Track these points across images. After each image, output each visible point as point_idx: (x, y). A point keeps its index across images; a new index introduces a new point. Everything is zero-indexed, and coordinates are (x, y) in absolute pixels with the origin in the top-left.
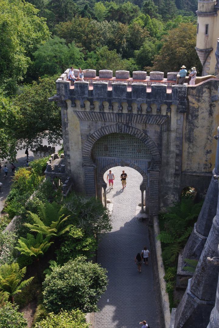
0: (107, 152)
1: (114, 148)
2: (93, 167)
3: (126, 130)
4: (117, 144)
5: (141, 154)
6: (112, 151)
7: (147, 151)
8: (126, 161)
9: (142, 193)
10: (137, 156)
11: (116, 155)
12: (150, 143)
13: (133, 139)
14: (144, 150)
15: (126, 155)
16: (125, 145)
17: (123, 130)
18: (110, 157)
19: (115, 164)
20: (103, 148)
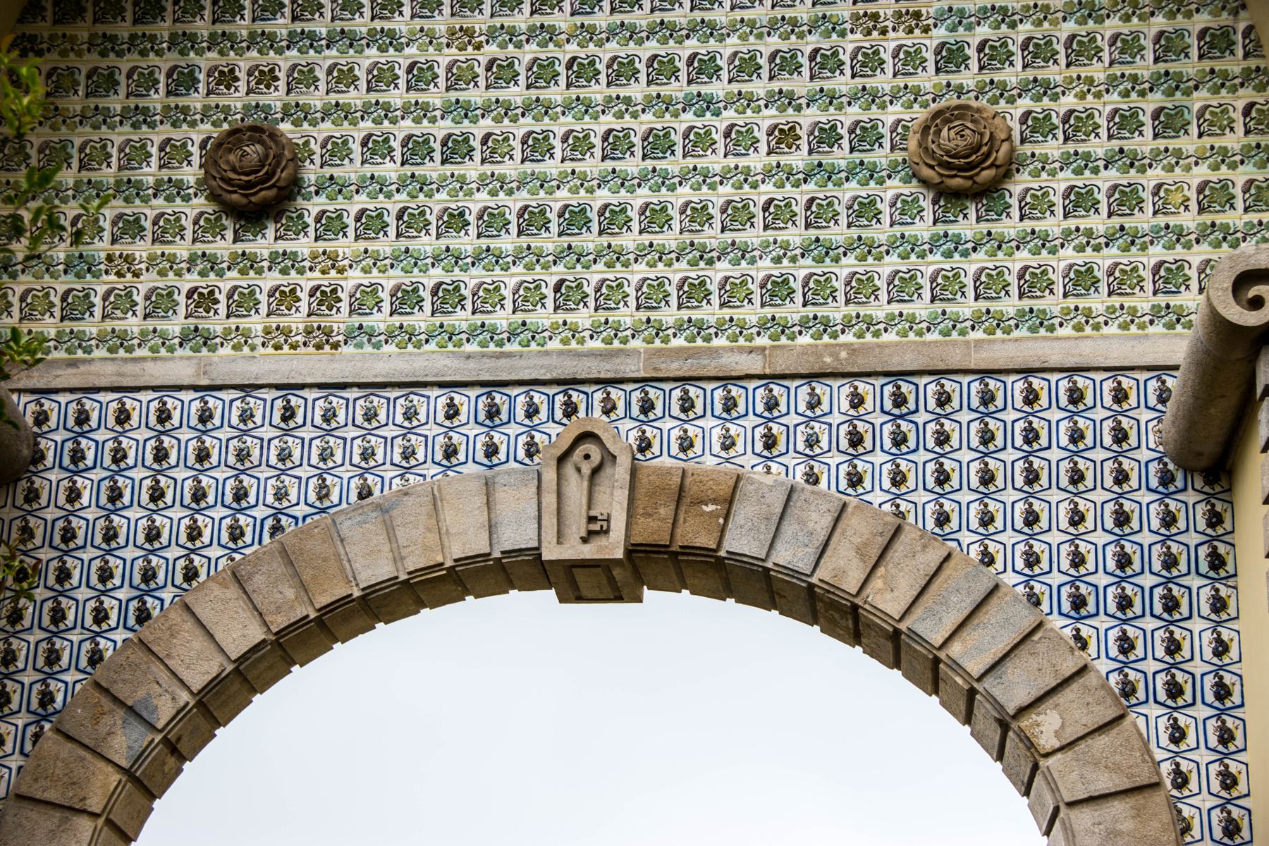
0: (264, 244)
4: (502, 72)
5: (1010, 226)
7: (1144, 143)
14: (1076, 125)
18: (324, 339)
20: (190, 174)
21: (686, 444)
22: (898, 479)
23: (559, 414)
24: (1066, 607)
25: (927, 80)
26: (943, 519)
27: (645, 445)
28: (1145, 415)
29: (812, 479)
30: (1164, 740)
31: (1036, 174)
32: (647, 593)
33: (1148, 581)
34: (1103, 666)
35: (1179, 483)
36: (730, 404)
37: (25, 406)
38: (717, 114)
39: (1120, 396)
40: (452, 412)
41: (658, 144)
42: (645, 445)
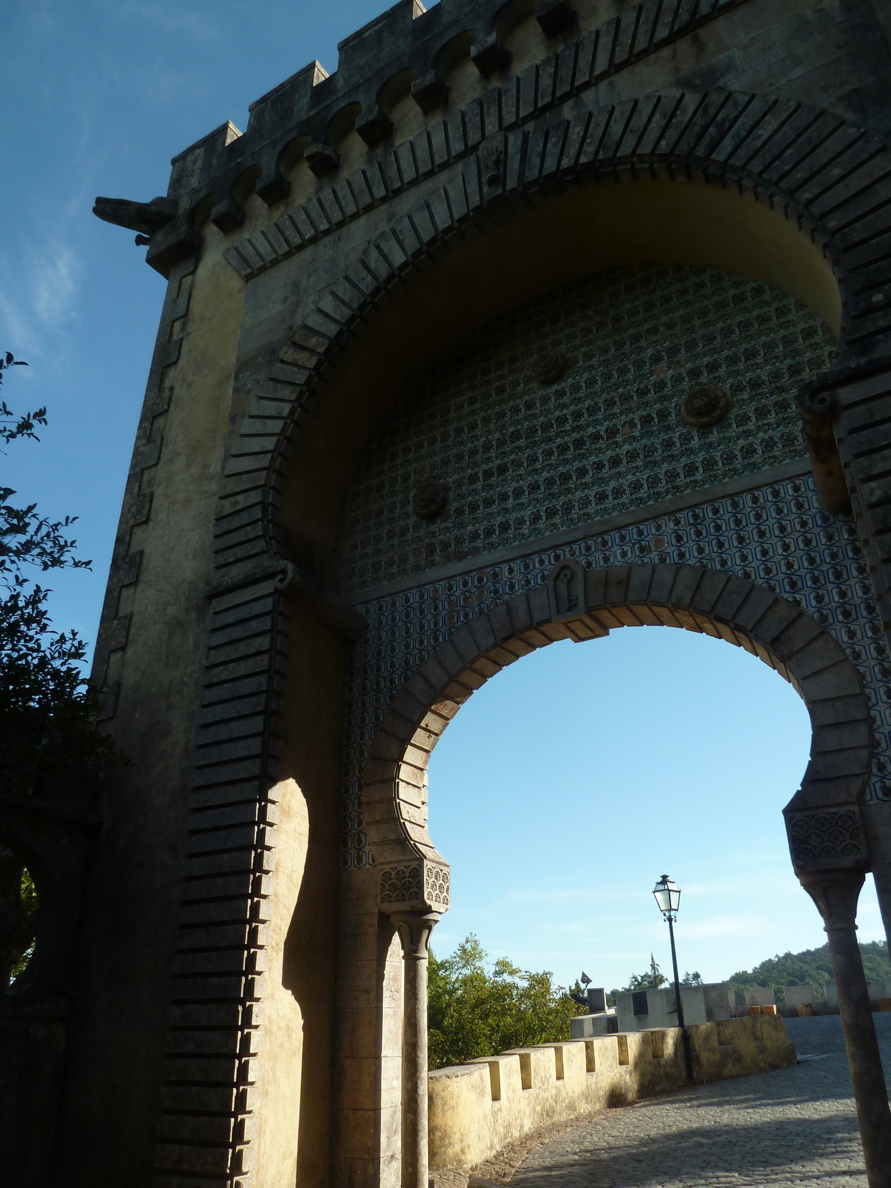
1: (488, 474)
2: (267, 587)
3: (537, 161)
4: (516, 436)
5: (734, 430)
6: (474, 508)
8: (597, 559)
9: (826, 910)
10: (691, 469)
11: (504, 527)
12: (772, 122)
13: (636, 338)
15: (592, 492)
16: (577, 415)
17: (514, 166)
18: (460, 556)
19: (504, 608)
20: (410, 508)
21: (606, 559)
22: (701, 550)
23: (553, 561)
24: (788, 588)
25: (686, 385)
26: (724, 563)
27: (589, 564)
28: (810, 494)
29: (663, 560)
30: (845, 638)
31: (740, 407)
32: (611, 631)
33: (825, 567)
34: (811, 610)
35: (832, 520)
36: (622, 538)
37: (361, 609)
38: (602, 425)
39: (796, 489)
40: (511, 571)
41: (579, 443)
42: (589, 564)
